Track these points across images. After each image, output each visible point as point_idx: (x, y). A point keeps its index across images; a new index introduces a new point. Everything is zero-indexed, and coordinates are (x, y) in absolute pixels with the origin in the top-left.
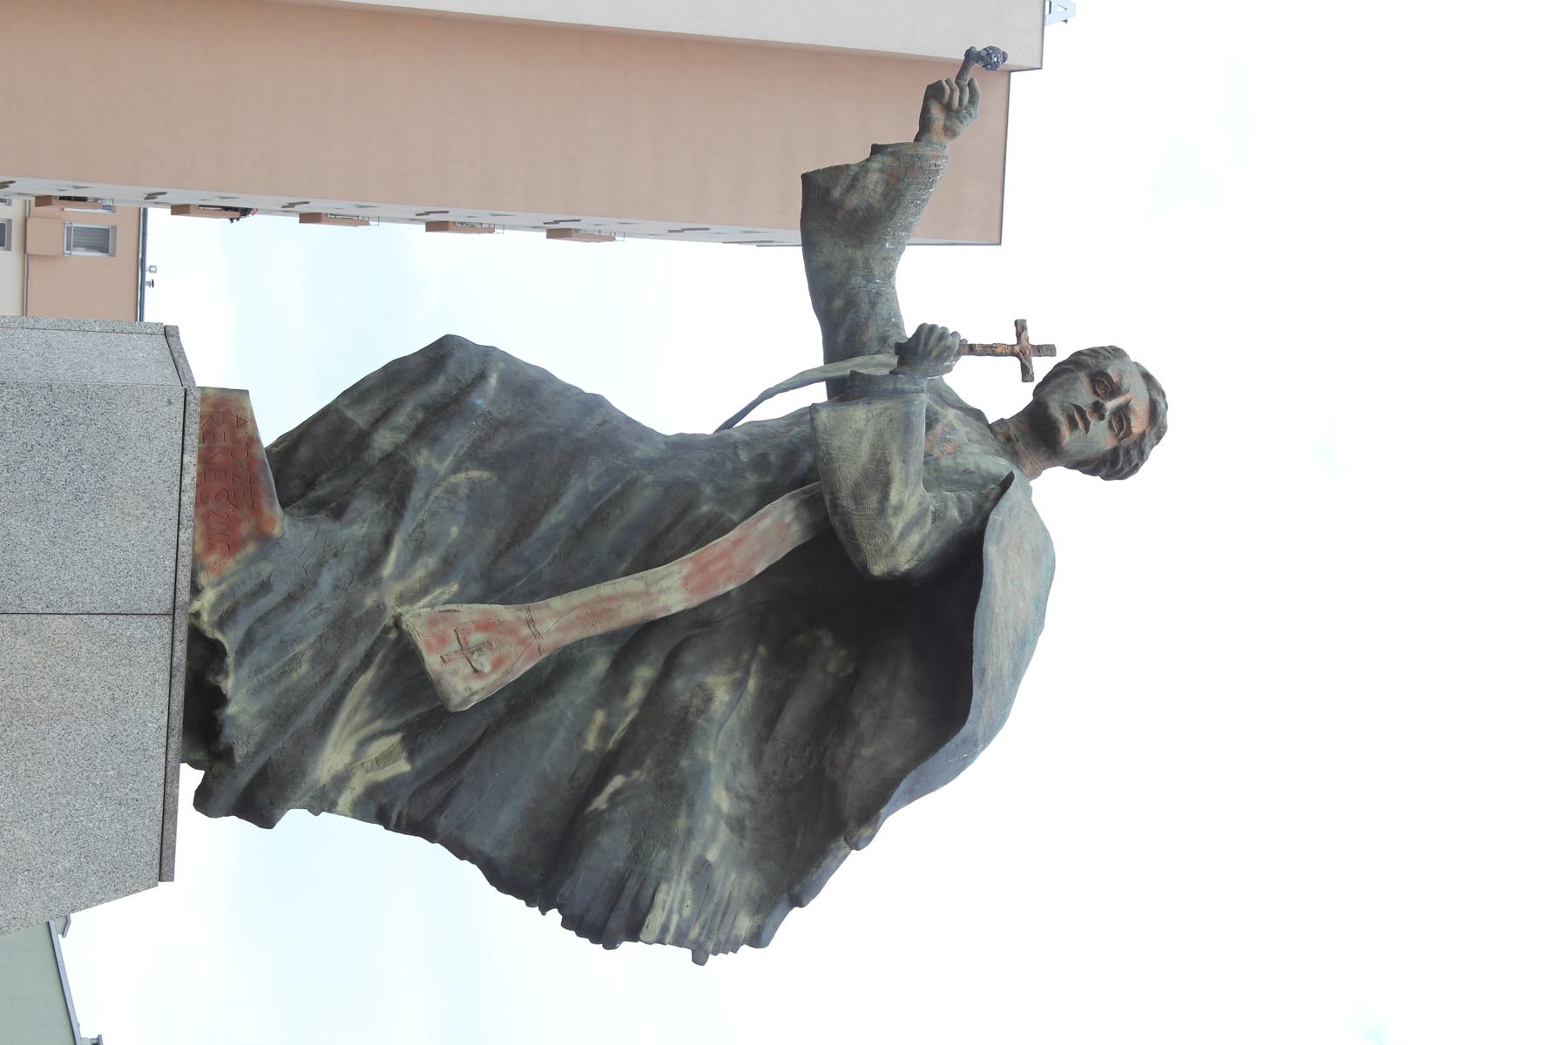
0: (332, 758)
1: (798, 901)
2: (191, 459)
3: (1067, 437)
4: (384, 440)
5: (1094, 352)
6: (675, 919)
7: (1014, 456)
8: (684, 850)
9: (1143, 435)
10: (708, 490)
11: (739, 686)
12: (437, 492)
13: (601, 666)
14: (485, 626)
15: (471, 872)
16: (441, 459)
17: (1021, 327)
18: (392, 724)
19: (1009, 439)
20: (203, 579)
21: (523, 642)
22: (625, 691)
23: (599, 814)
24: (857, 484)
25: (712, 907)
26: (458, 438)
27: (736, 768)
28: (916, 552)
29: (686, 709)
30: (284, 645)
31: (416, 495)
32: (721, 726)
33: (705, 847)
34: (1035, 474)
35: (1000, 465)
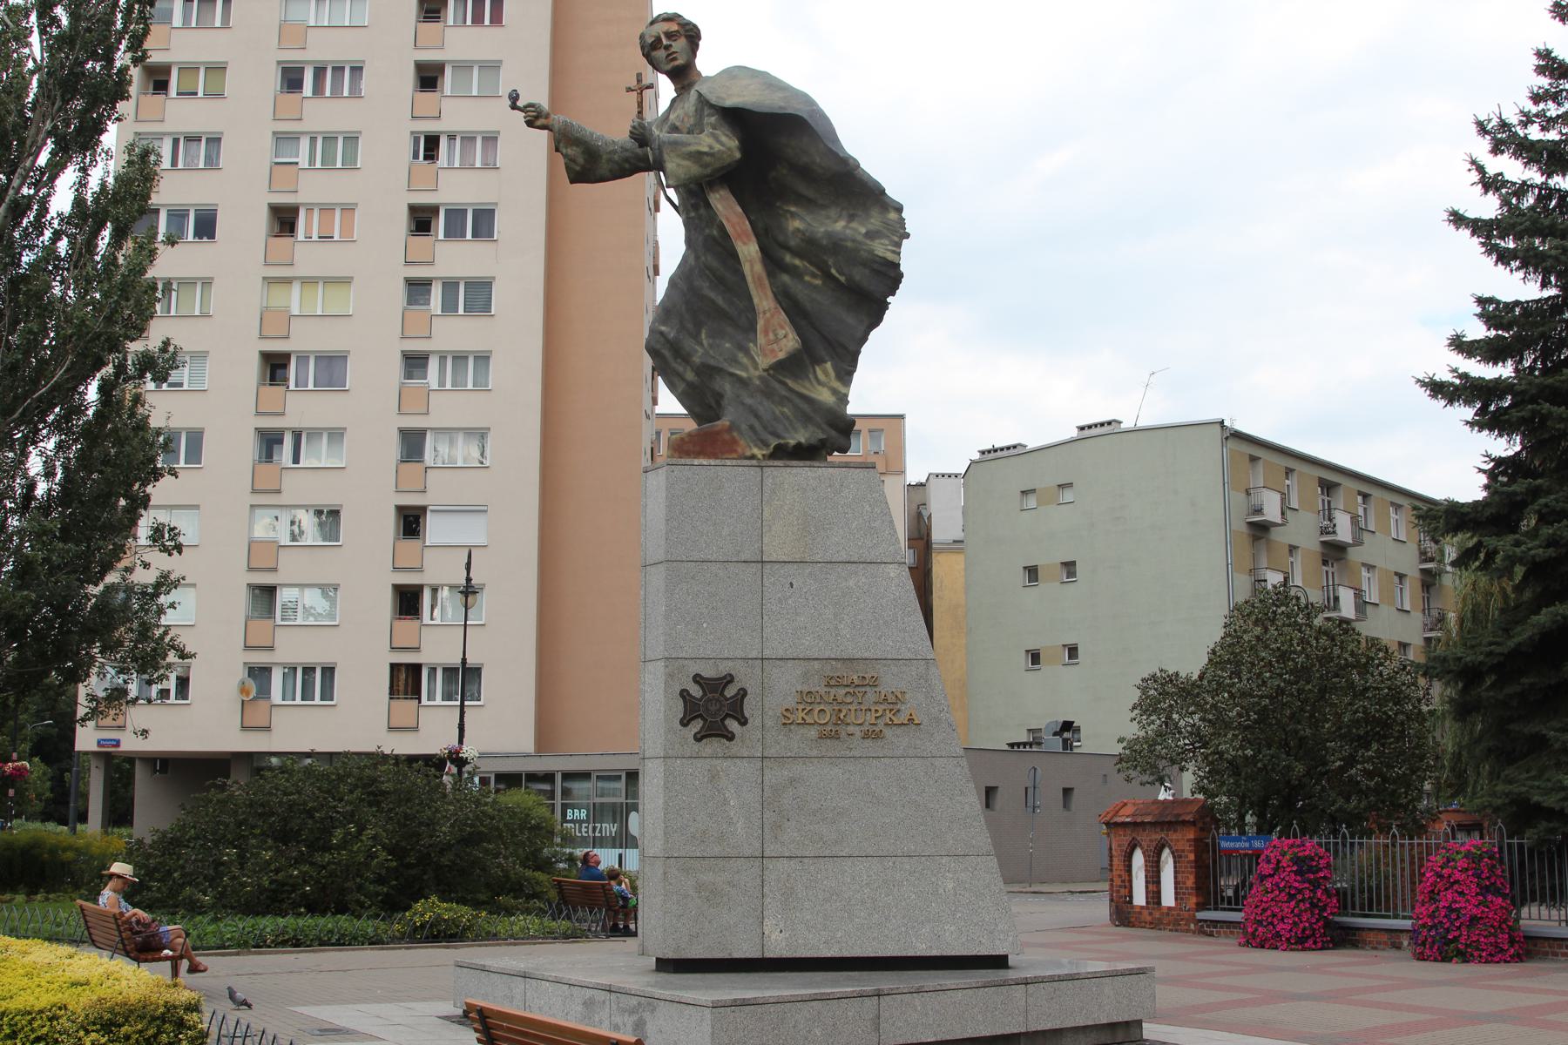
0: (825, 396)
1: (883, 192)
2: (696, 462)
3: (680, 62)
4: (690, 376)
5: (643, 48)
6: (890, 248)
7: (691, 85)
8: (860, 243)
9: (679, 24)
10: (707, 231)
11: (793, 215)
12: (711, 352)
13: (786, 278)
14: (766, 333)
15: (874, 334)
16: (696, 351)
17: (629, 90)
18: (811, 370)
19: (683, 88)
20: (748, 453)
21: (772, 316)
22: (796, 267)
23: (847, 279)
24: (701, 166)
25: (885, 231)
26: (688, 344)
27: (828, 217)
28: (730, 138)
29: (802, 240)
30: (776, 419)
31: (712, 362)
32: (809, 224)
33: (860, 233)
34: (699, 74)
35: (693, 96)
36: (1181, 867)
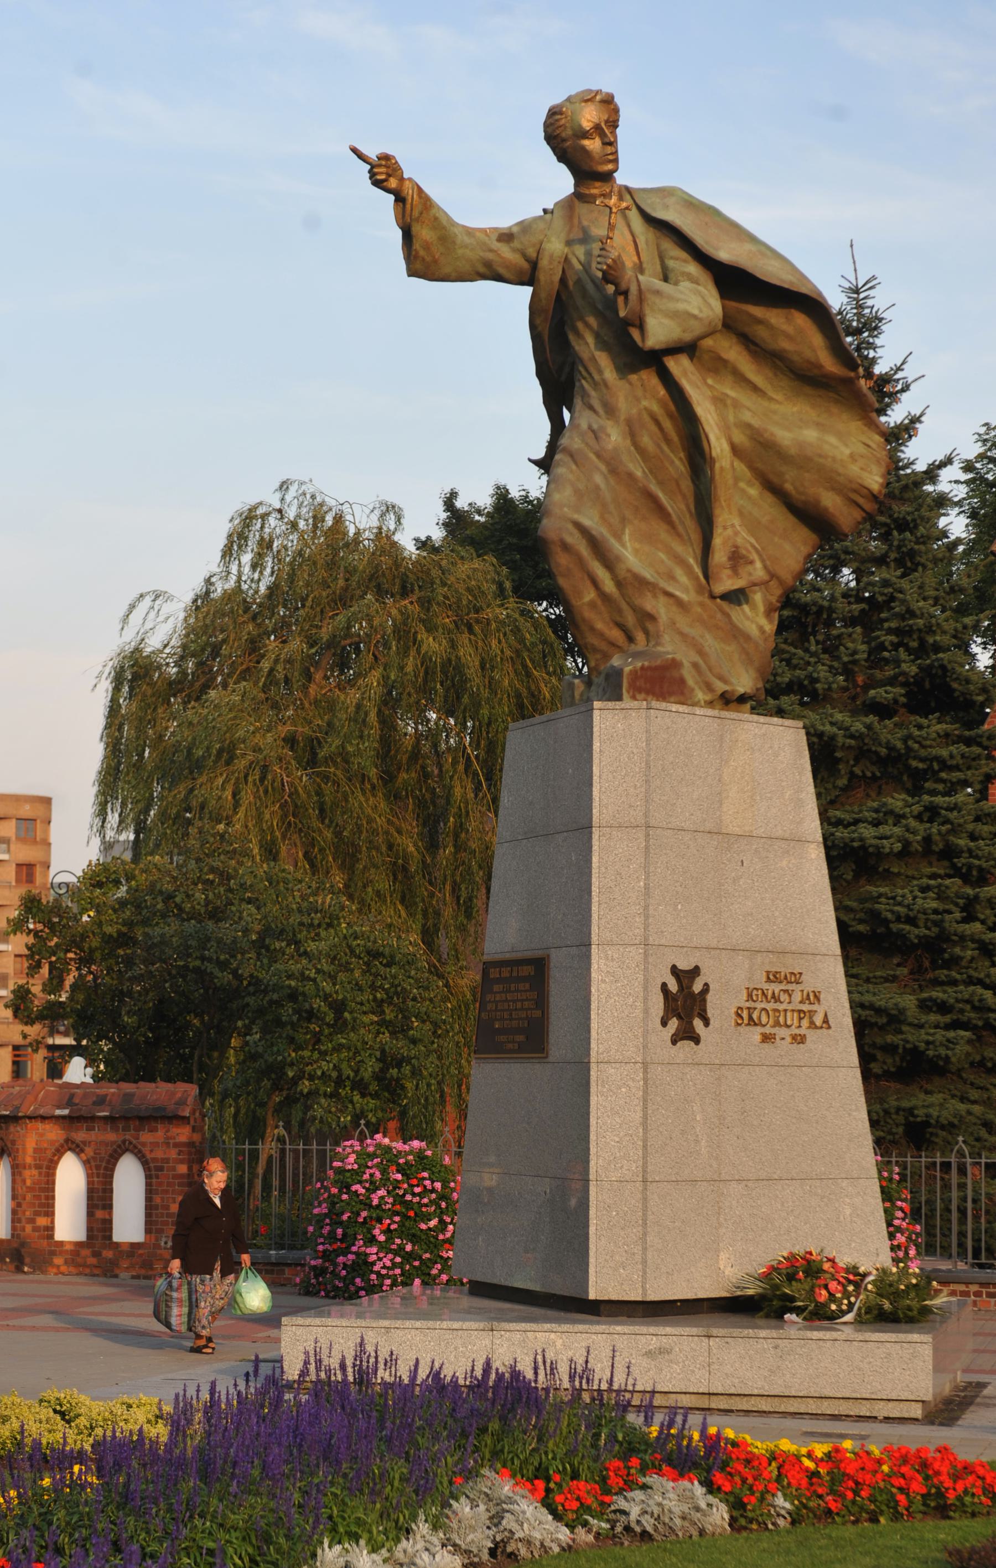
4: (609, 586)
36: (160, 1184)
